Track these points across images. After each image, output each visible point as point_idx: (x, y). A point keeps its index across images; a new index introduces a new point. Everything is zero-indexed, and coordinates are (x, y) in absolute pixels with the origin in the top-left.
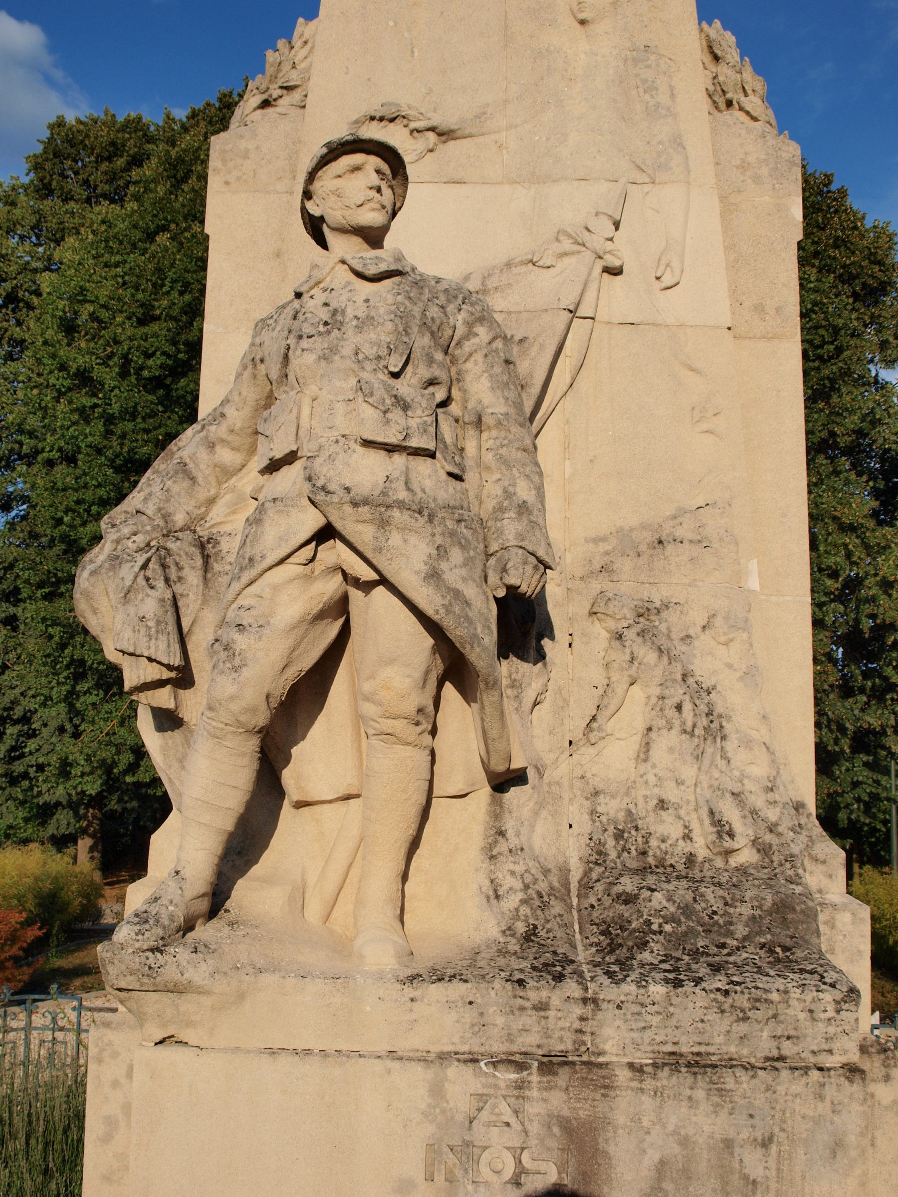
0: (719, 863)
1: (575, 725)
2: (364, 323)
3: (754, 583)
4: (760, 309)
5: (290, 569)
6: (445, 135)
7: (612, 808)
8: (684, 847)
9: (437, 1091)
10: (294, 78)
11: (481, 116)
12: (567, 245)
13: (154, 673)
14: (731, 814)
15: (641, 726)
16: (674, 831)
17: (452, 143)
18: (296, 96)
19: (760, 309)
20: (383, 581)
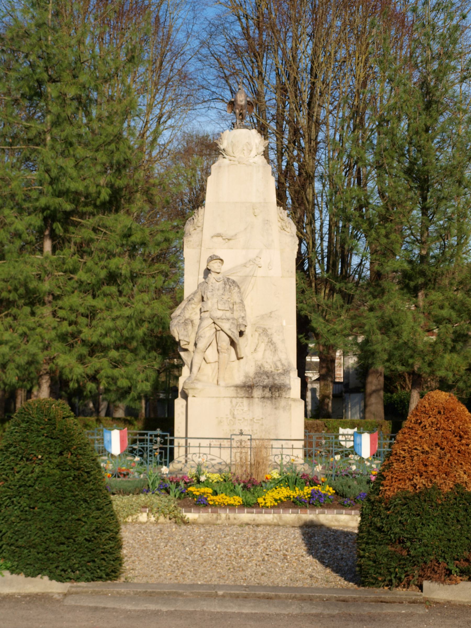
0: (276, 372)
1: (253, 350)
2: (218, 290)
3: (284, 324)
4: (288, 271)
5: (208, 328)
6: (229, 240)
7: (259, 363)
8: (271, 369)
9: (231, 402)
10: (199, 224)
11: (236, 235)
12: (251, 263)
13: (186, 343)
14: (279, 364)
15: (263, 349)
16: (269, 367)
17: (230, 241)
18: (200, 228)
19: (288, 271)
20: (222, 330)
